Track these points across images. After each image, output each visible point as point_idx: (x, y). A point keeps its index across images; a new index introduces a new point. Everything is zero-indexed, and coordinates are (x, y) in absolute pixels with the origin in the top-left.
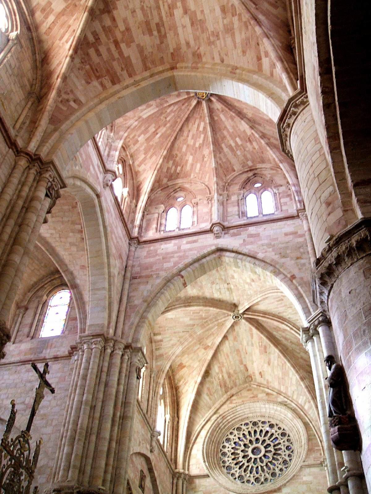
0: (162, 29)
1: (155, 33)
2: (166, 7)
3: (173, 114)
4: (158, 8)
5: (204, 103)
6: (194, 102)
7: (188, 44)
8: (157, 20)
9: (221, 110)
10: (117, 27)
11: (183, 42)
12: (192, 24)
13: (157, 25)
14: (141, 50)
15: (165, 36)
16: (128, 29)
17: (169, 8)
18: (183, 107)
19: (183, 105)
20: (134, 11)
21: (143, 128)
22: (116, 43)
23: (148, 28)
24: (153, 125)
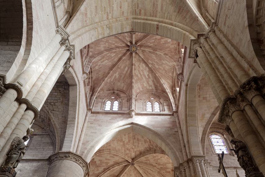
0: (133, 137)
1: (136, 138)
2: (130, 142)
3: (151, 41)
4: (133, 142)
5: (134, 43)
6: (138, 44)
7: (125, 135)
8: (134, 140)
9: (126, 37)
10: (149, 144)
11: (127, 136)
12: (122, 140)
13: (135, 139)
14: (143, 137)
15: (133, 136)
16: (145, 142)
17: (129, 142)
18: (145, 42)
19: (145, 43)
20: (142, 144)
21: (167, 45)
22: (150, 142)
23: (138, 140)
24: (161, 43)
